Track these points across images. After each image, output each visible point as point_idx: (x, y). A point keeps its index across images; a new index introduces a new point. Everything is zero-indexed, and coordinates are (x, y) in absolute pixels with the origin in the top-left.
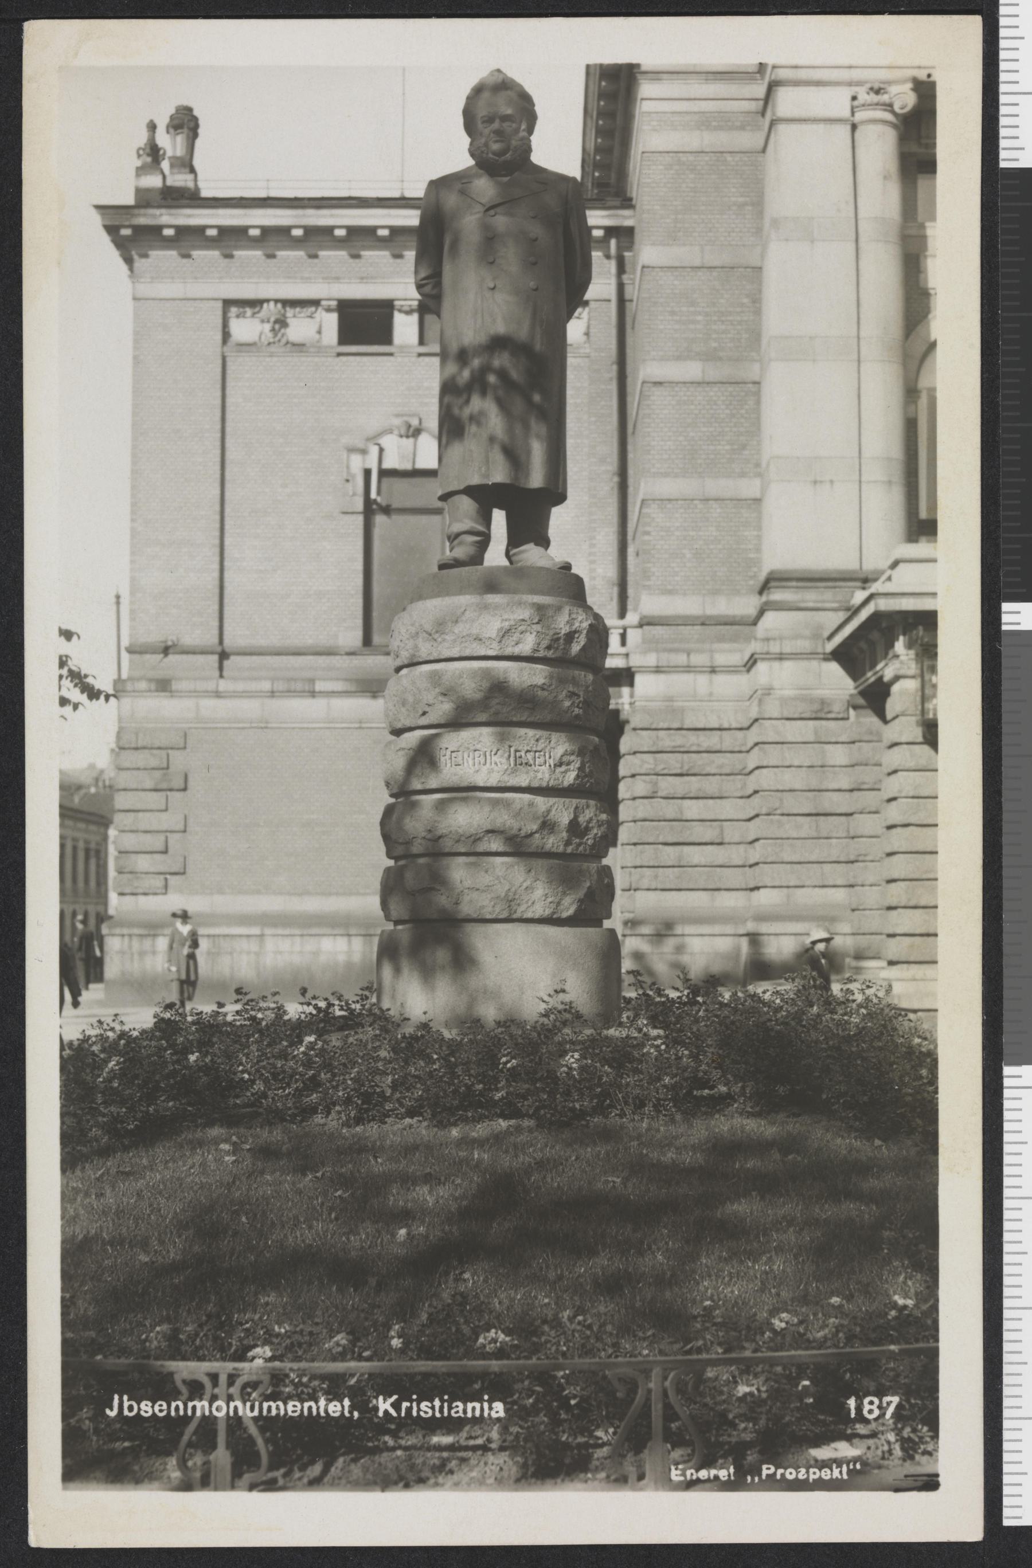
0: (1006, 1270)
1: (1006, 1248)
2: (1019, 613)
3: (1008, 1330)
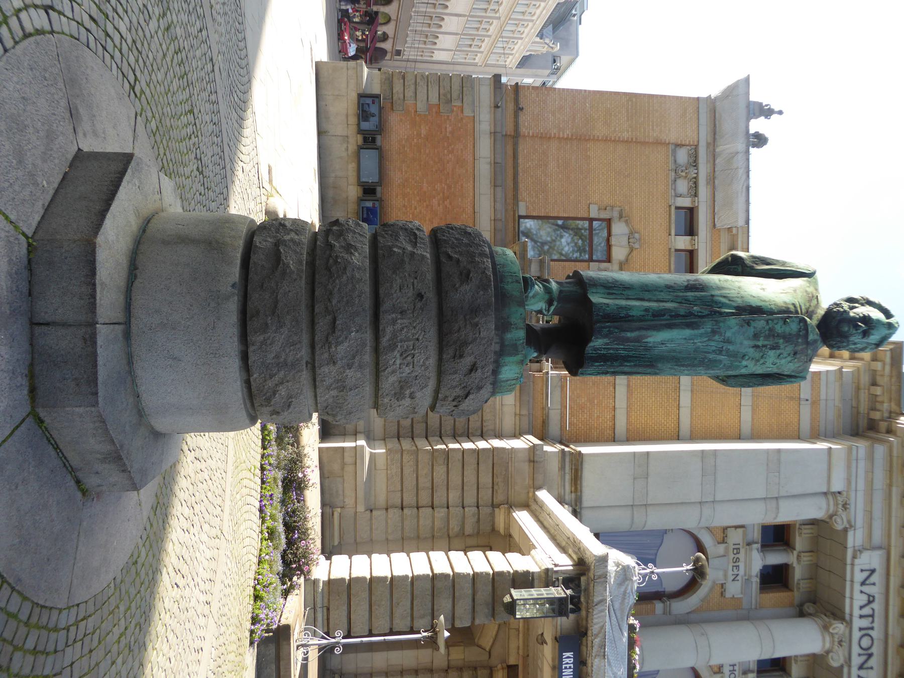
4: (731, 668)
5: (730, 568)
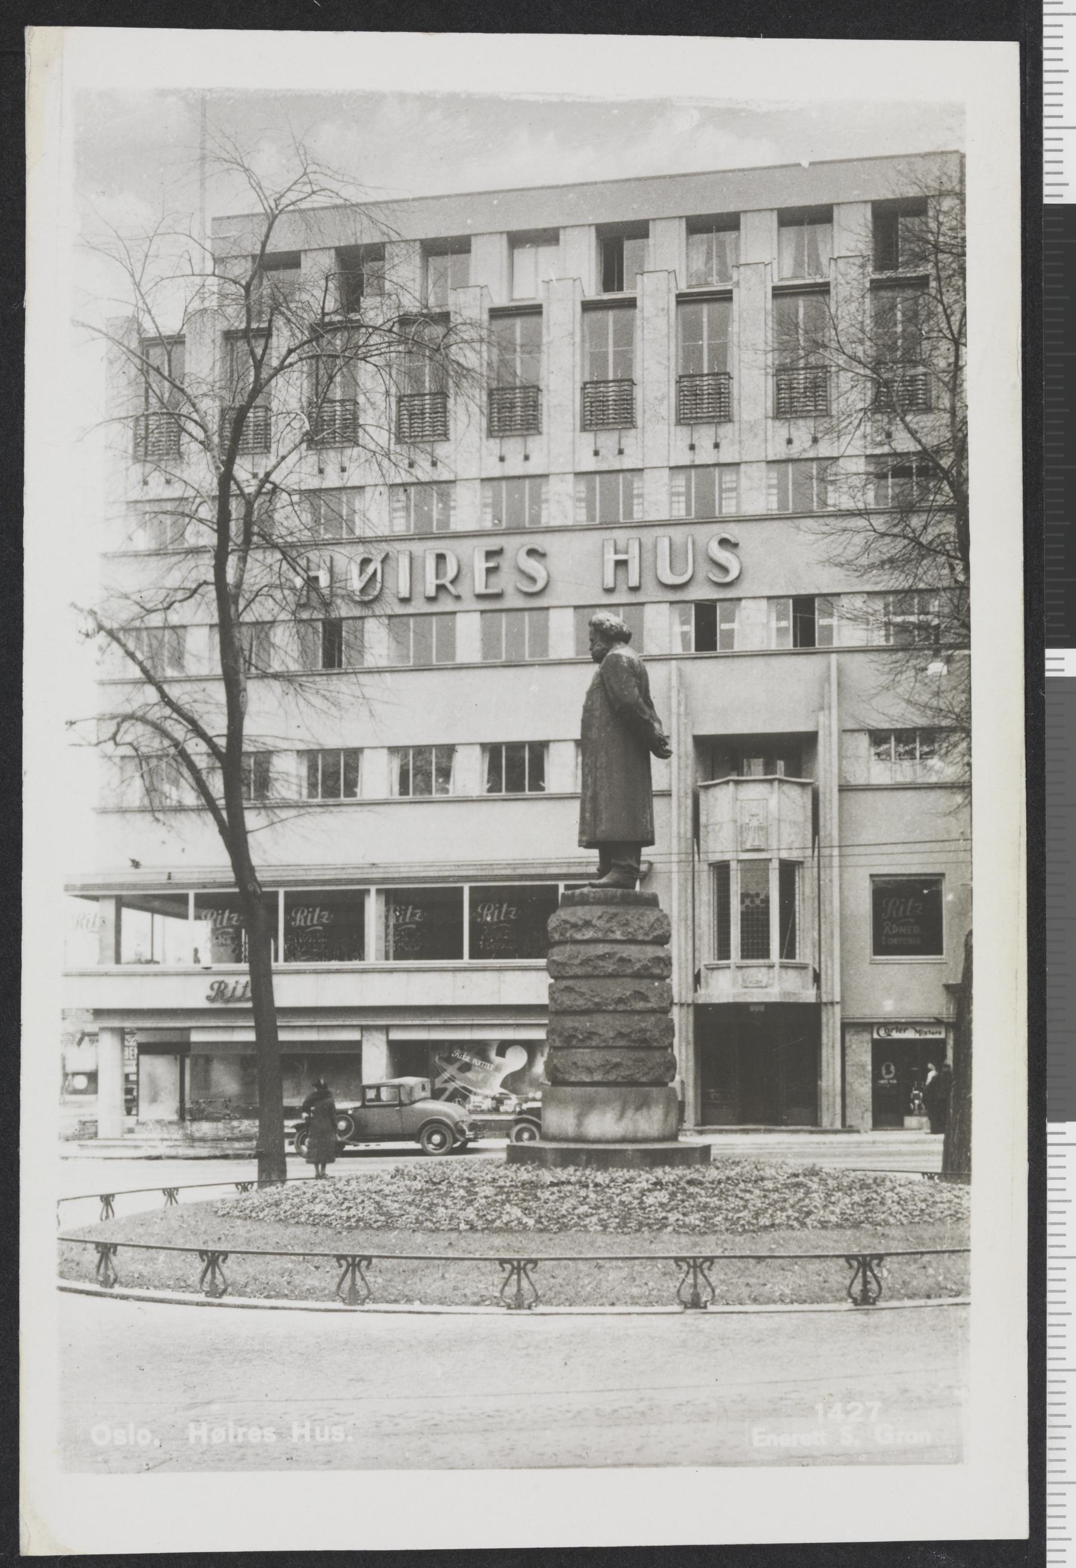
0: (1050, 1331)
1: (1050, 1308)
2: (1063, 659)
3: (1052, 1393)
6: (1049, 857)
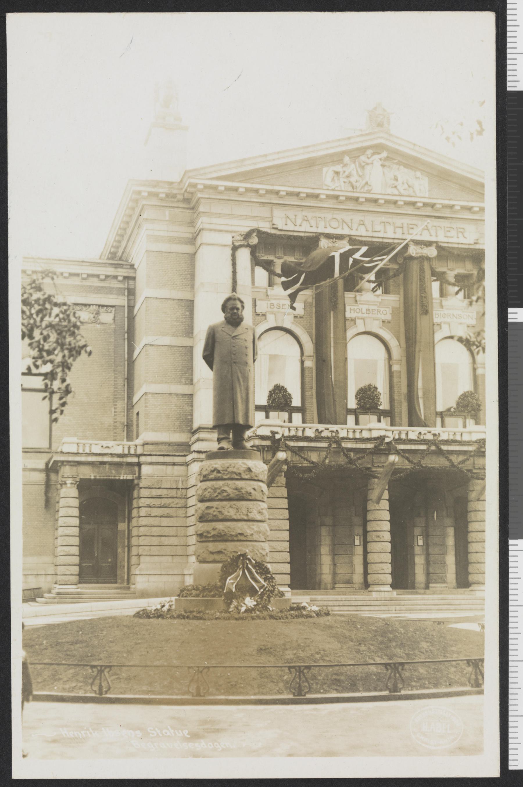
0: (510, 642)
1: (510, 631)
2: (517, 313)
3: (511, 672)
4: (352, 312)
5: (283, 310)
6: (510, 410)
